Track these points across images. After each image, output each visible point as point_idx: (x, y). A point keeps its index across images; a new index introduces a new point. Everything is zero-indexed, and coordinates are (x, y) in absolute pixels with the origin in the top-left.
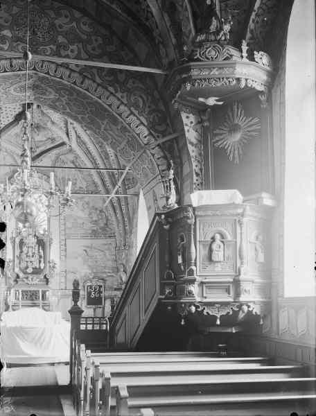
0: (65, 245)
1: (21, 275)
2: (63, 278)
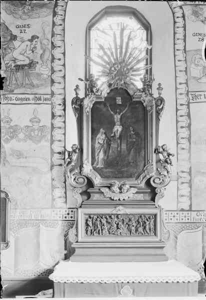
0: (189, 115)
1: (97, 180)
2: (186, 185)
